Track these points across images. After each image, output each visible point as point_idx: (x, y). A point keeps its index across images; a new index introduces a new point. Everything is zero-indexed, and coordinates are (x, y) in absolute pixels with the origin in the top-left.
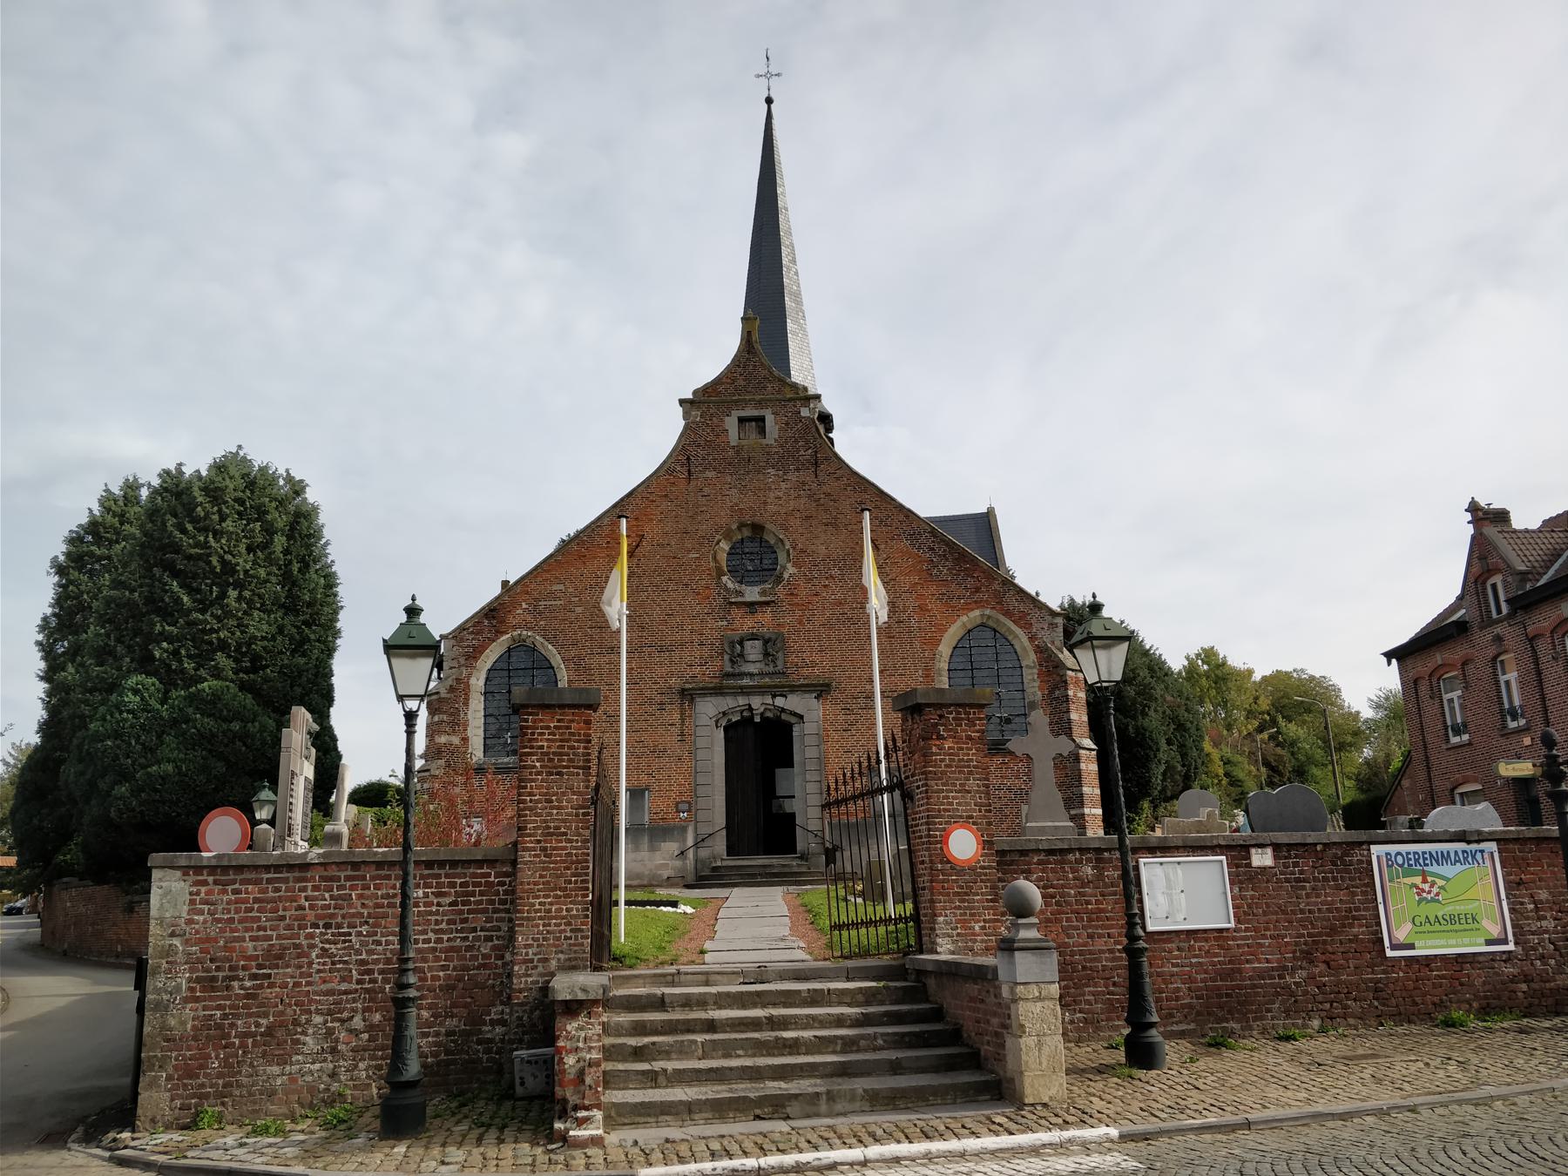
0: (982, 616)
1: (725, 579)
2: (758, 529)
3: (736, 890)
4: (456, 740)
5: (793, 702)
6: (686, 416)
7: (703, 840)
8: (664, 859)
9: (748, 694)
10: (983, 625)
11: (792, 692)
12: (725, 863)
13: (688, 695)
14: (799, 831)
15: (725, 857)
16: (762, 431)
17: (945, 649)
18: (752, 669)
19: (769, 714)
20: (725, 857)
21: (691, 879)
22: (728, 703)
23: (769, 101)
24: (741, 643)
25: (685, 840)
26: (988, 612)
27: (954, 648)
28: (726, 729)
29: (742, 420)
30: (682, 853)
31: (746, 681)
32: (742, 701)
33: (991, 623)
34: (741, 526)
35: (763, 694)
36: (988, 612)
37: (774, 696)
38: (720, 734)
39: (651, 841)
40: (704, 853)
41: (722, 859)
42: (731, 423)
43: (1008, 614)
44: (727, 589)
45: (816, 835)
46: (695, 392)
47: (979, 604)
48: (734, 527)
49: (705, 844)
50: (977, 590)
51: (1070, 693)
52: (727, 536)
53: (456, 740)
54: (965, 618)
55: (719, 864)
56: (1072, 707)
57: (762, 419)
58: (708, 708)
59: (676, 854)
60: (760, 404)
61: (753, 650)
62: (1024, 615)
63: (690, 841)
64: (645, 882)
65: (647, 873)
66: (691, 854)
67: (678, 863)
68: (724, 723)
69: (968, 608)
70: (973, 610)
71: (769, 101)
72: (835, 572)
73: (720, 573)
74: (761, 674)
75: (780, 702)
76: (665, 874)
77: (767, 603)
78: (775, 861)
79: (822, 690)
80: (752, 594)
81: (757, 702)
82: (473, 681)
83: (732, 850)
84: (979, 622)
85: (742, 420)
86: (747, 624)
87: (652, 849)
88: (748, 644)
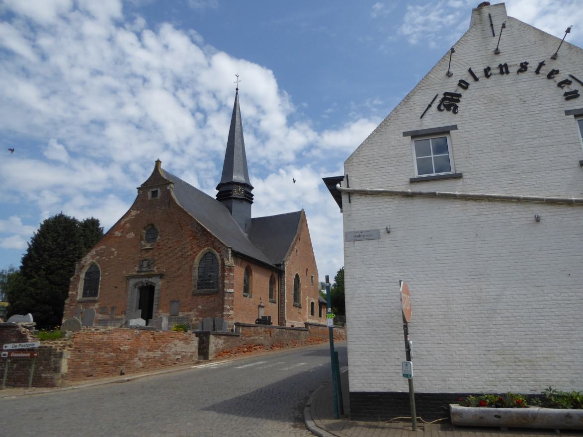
0: (208, 249)
1: (142, 242)
2: (152, 225)
4: (74, 293)
5: (152, 280)
6: (138, 192)
9: (143, 277)
10: (210, 252)
11: (153, 276)
13: (128, 278)
16: (157, 196)
17: (197, 261)
18: (144, 269)
19: (149, 284)
22: (137, 280)
23: (237, 89)
24: (142, 262)
25: (122, 322)
26: (209, 248)
27: (201, 260)
28: (138, 288)
29: (153, 192)
31: (143, 274)
32: (140, 280)
33: (211, 251)
34: (148, 225)
35: (146, 277)
36: (209, 248)
37: (149, 278)
38: (137, 290)
42: (149, 194)
43: (215, 248)
44: (142, 245)
46: (142, 185)
47: (207, 245)
48: (146, 225)
50: (207, 241)
51: (226, 274)
52: (145, 229)
53: (74, 293)
54: (203, 250)
56: (226, 278)
57: (157, 191)
58: (132, 282)
60: (157, 187)
61: (145, 264)
62: (219, 248)
68: (137, 287)
69: (204, 247)
70: (205, 247)
71: (237, 89)
72: (170, 237)
73: (142, 239)
74: (147, 271)
75: (150, 280)
77: (151, 249)
79: (161, 276)
80: (148, 246)
81: (144, 280)
82: (81, 276)
84: (208, 251)
85: (153, 192)
86: (145, 255)
88: (145, 261)
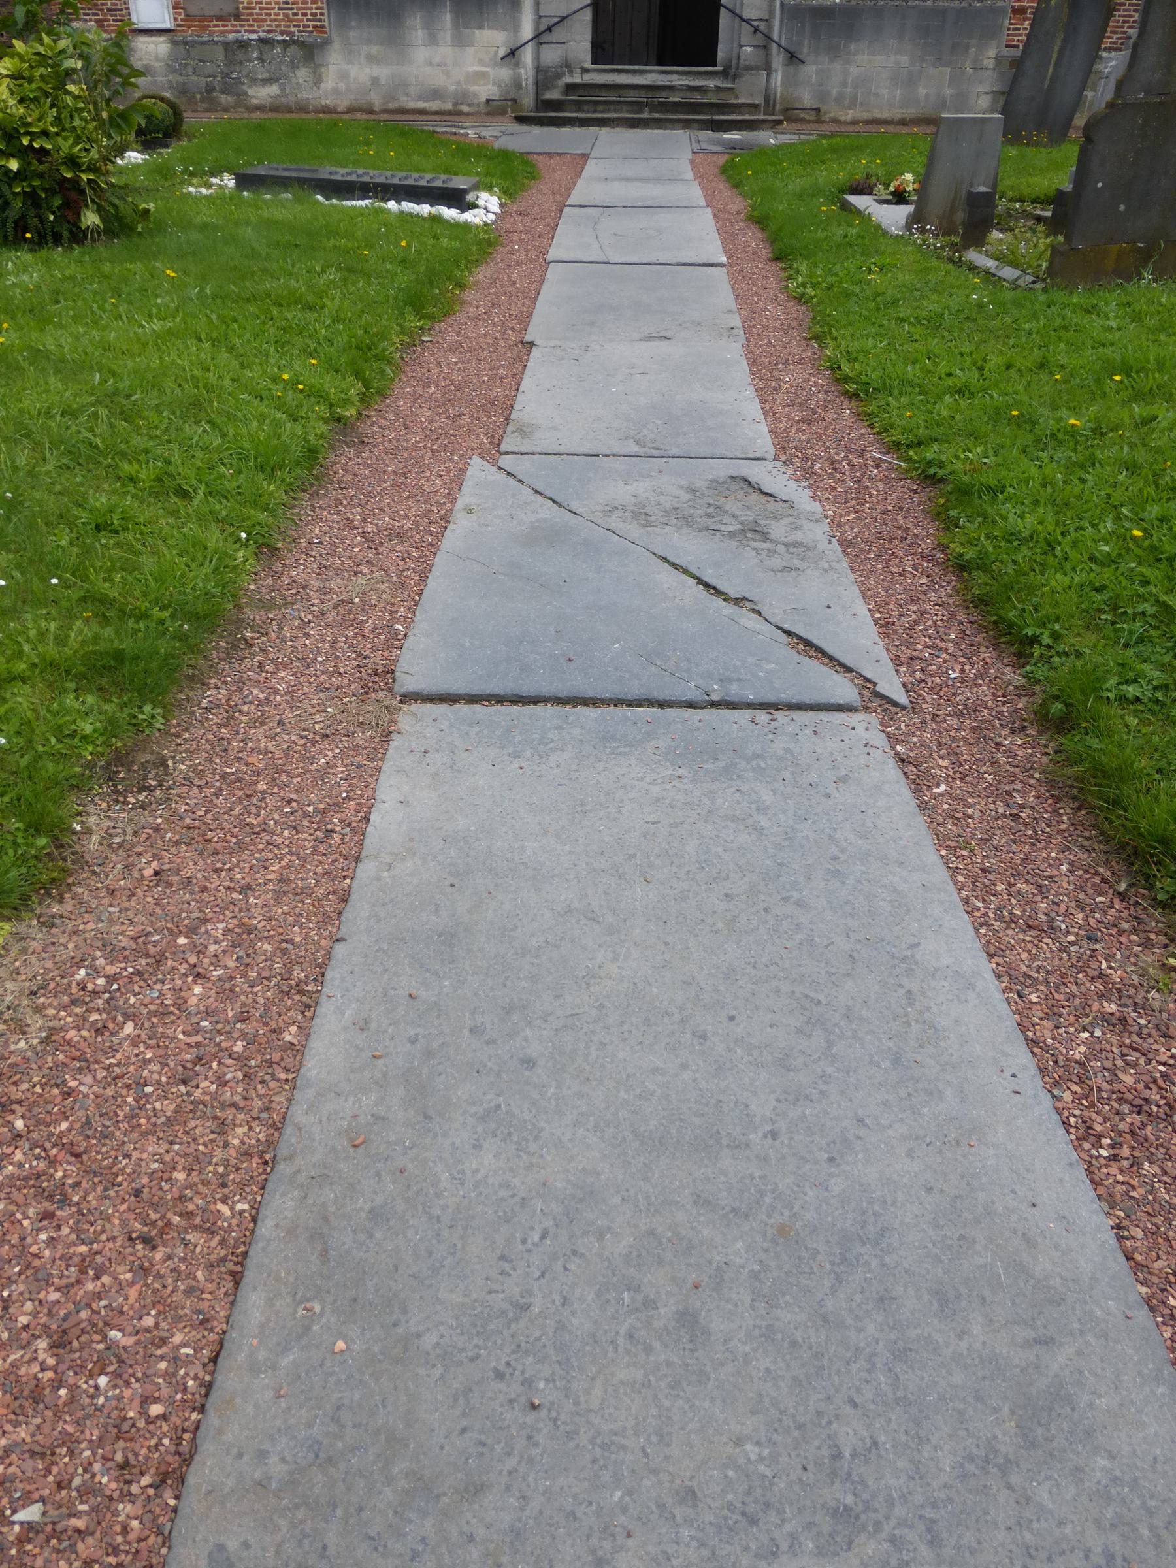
3: (604, 132)
7: (550, 29)
8: (481, 62)
12: (589, 78)
14: (724, 18)
15: (588, 65)
20: (588, 65)
21: (528, 101)
25: (516, 28)
30: (512, 53)
39: (456, 25)
40: (551, 56)
41: (585, 71)
45: (756, 30)
49: (557, 35)
55: (577, 79)
59: (502, 52)
63: (527, 30)
64: (449, 106)
65: (452, 88)
66: (527, 56)
67: (505, 73)
76: (485, 91)
78: (677, 78)
83: (602, 52)
87: (461, 43)
